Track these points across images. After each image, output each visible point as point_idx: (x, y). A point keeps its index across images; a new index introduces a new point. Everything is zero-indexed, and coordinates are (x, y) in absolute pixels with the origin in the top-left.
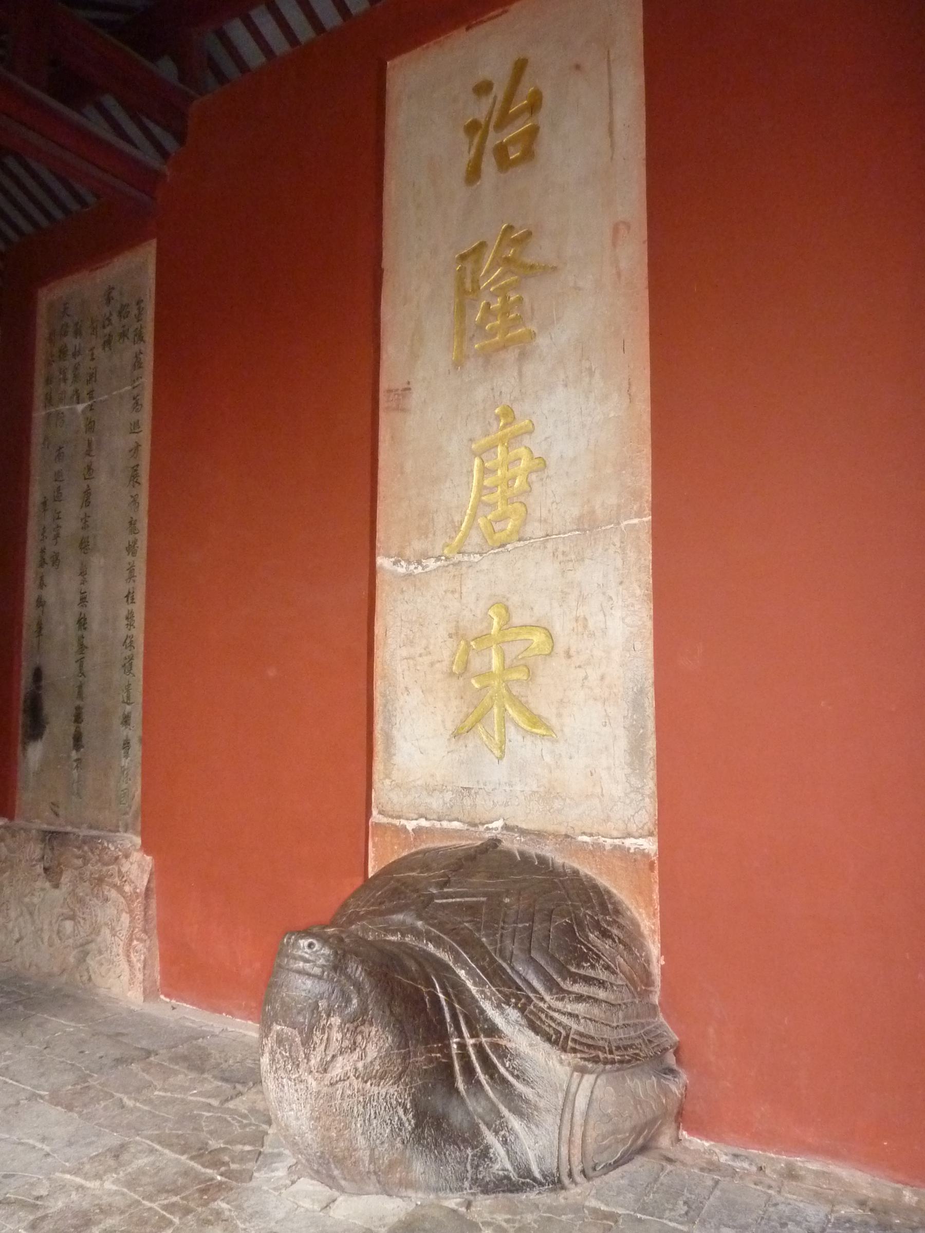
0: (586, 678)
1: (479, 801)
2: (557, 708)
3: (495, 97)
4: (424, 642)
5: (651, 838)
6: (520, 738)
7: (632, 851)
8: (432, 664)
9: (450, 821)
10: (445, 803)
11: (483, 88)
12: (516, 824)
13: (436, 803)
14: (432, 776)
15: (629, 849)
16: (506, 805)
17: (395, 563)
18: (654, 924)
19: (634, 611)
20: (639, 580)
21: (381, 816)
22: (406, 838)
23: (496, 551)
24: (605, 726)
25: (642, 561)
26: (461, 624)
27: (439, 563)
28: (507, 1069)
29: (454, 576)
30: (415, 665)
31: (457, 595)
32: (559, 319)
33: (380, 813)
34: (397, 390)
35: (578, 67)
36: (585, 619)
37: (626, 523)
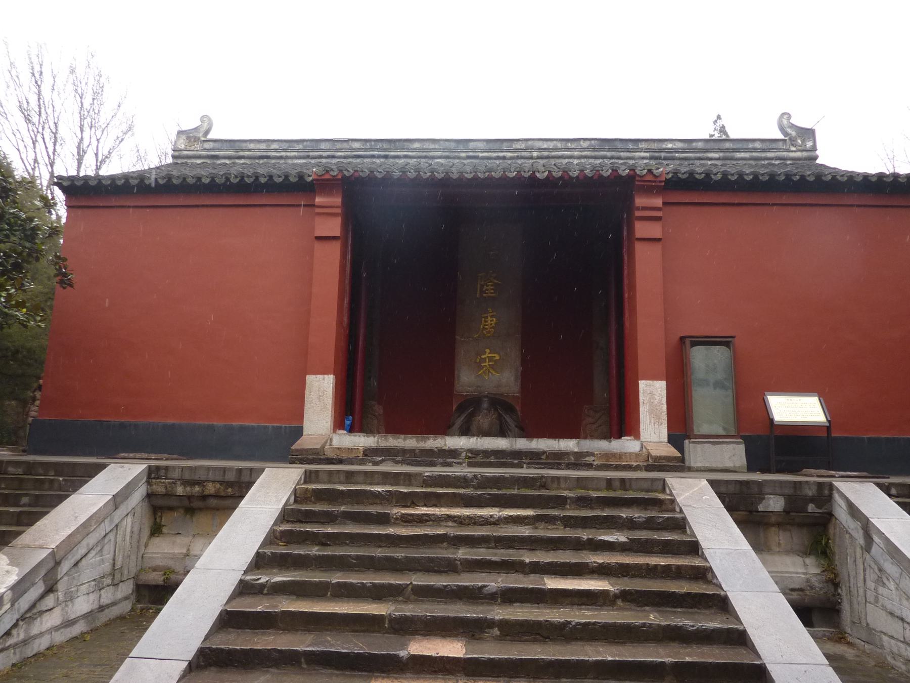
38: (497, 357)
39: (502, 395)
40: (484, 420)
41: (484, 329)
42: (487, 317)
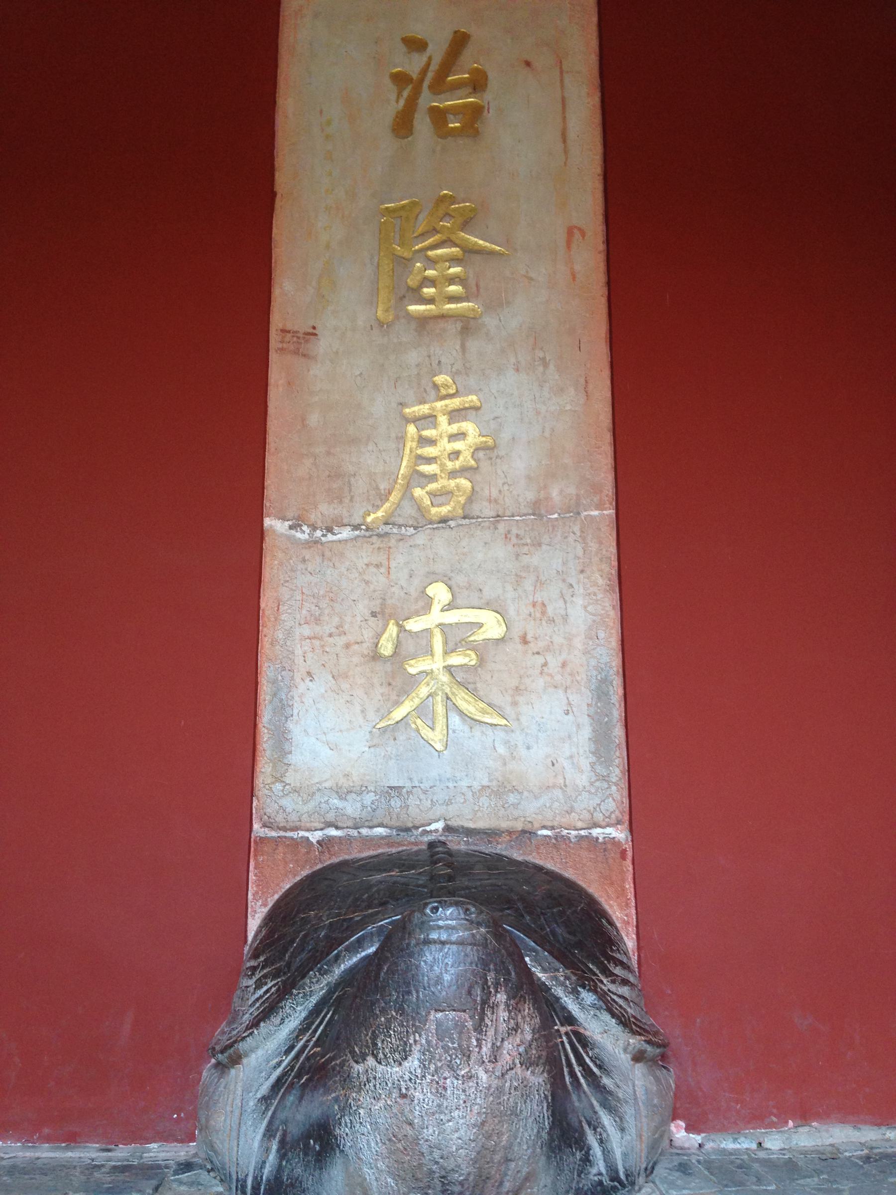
0: (545, 664)
1: (412, 801)
2: (513, 696)
3: (430, 58)
4: (336, 620)
5: (619, 826)
6: (466, 728)
7: (601, 840)
8: (347, 646)
9: (371, 827)
10: (364, 807)
11: (416, 45)
12: (461, 823)
13: (352, 808)
14: (347, 776)
15: (597, 838)
16: (448, 803)
17: (291, 528)
18: (626, 916)
19: (597, 600)
20: (601, 570)
21: (266, 829)
22: (308, 853)
23: (435, 526)
24: (567, 714)
25: (604, 552)
26: (389, 602)
27: (357, 533)
28: (591, 1058)
29: (379, 548)
30: (322, 646)
31: (382, 570)
32: (508, 303)
33: (265, 826)
34: (297, 332)
35: (528, 64)
36: (543, 605)
37: (586, 513)
38: (492, 626)
39: (526, 834)
40: (442, 1088)
41: (418, 478)
42: (430, 419)
